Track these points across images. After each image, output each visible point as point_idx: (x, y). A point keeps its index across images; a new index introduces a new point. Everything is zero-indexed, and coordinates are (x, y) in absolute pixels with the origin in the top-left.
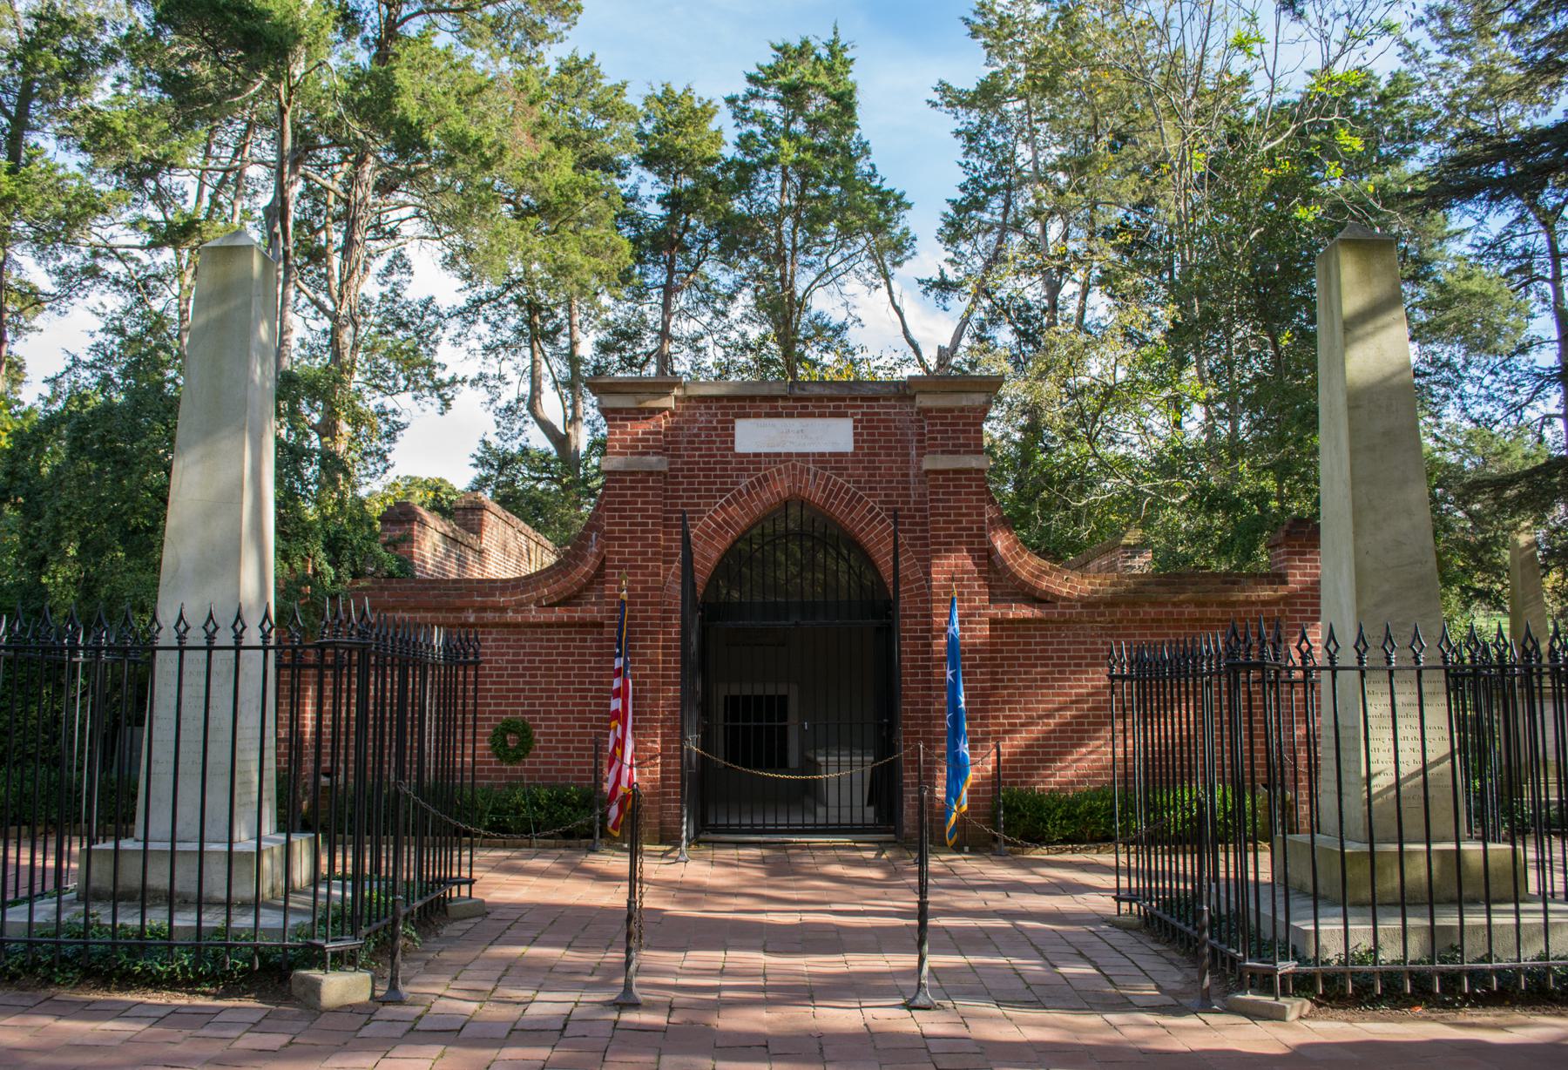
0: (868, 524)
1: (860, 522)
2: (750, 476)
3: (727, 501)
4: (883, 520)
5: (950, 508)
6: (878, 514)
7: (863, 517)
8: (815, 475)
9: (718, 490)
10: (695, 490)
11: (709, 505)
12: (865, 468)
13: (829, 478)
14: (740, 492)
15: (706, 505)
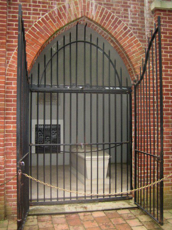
0: (124, 36)
1: (119, 34)
2: (59, 4)
3: (46, 17)
4: (132, 35)
5: (167, 29)
6: (129, 31)
7: (122, 32)
8: (96, 6)
9: (40, 10)
10: (27, 9)
11: (36, 18)
12: (122, 6)
13: (103, 9)
14: (53, 12)
15: (33, 18)
